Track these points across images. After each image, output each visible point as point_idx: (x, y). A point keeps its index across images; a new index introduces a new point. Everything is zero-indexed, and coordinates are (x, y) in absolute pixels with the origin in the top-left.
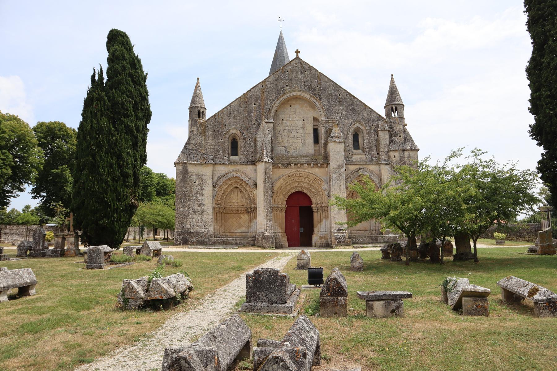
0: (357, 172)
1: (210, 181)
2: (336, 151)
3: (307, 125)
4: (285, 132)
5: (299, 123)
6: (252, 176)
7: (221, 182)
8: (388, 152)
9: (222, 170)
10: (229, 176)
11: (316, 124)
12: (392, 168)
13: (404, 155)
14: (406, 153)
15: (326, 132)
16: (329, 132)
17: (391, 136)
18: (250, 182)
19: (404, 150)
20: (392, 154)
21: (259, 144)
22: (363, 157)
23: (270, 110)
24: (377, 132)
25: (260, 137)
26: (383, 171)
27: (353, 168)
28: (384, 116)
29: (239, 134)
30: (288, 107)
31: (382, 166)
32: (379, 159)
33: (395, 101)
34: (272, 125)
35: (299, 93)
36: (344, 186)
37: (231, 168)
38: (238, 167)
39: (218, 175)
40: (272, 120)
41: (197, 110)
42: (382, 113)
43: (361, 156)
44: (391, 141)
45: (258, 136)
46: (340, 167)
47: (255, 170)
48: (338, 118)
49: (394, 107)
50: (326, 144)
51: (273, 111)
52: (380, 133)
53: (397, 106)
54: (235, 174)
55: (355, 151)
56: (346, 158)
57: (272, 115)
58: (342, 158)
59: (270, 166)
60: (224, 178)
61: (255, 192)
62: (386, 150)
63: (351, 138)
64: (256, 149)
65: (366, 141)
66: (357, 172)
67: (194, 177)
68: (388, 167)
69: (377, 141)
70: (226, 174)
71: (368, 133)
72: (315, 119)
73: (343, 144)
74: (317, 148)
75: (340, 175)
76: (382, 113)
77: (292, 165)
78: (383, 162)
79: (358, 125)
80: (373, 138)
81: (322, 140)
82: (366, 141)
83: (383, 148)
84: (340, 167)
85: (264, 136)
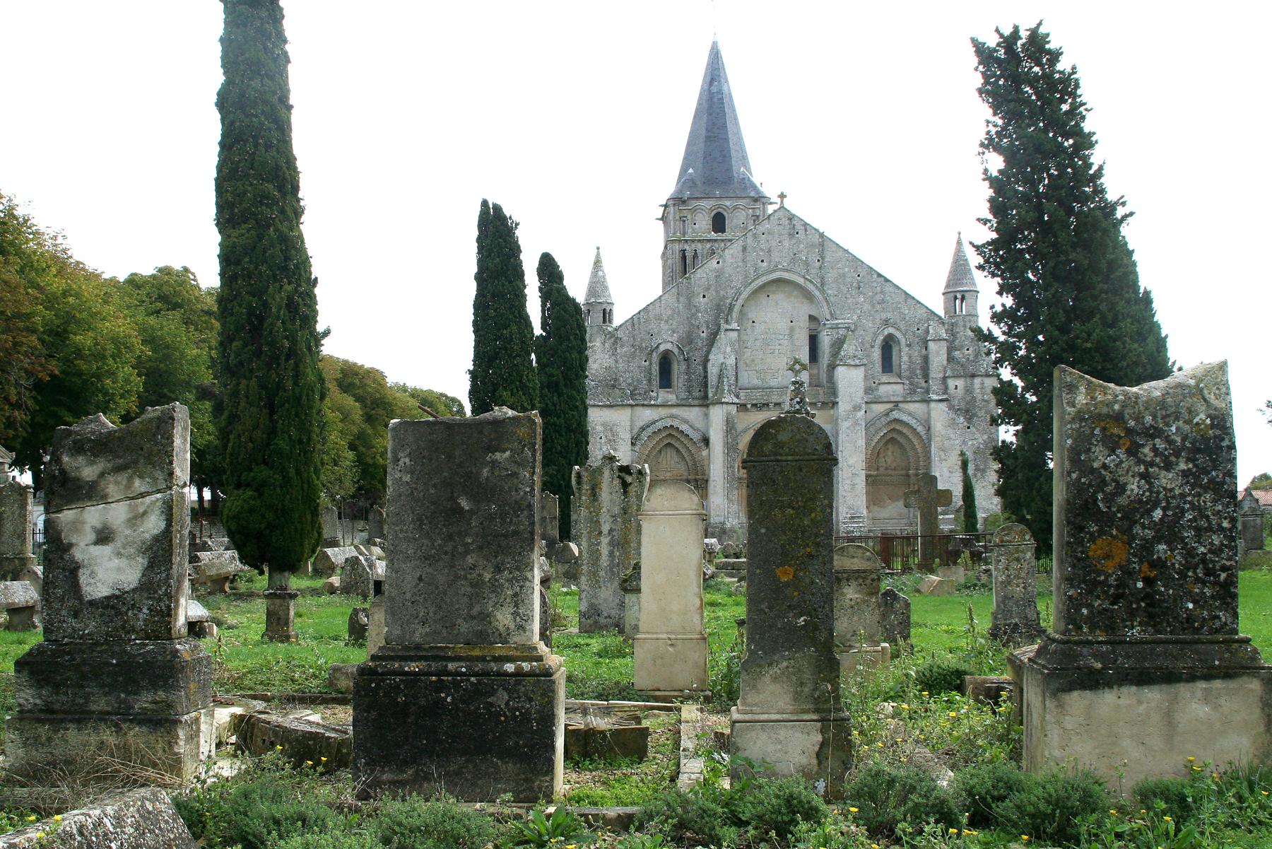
0: (887, 415)
1: (628, 436)
2: (850, 381)
3: (797, 330)
4: (758, 343)
5: (783, 325)
6: (699, 424)
7: (644, 436)
8: (945, 378)
9: (647, 415)
10: (659, 425)
11: (813, 326)
12: (951, 408)
13: (972, 384)
14: (977, 381)
15: (832, 346)
16: (838, 344)
17: (950, 350)
18: (695, 436)
19: (973, 376)
20: (951, 383)
21: (713, 370)
22: (899, 388)
23: (731, 307)
24: (925, 343)
25: (716, 359)
26: (933, 414)
27: (879, 408)
28: (941, 313)
29: (676, 351)
30: (762, 297)
31: (933, 405)
32: (927, 391)
33: (961, 284)
34: (735, 334)
35: (786, 275)
36: (861, 442)
37: (663, 412)
38: (675, 411)
39: (640, 424)
40: (734, 325)
41: (600, 308)
42: (938, 306)
43: (894, 386)
44: (950, 359)
45: (711, 357)
46: (856, 408)
47: (706, 415)
48: (855, 317)
49: (959, 296)
50: (832, 367)
51: (737, 309)
52: (931, 345)
53: (967, 295)
54: (669, 423)
55: (885, 378)
56: (868, 390)
57: (735, 315)
58: (861, 393)
59: (733, 409)
60: (650, 430)
61: (704, 453)
62: (941, 375)
63: (877, 354)
64: (706, 377)
65: (905, 358)
66: (887, 415)
67: (599, 428)
68: (943, 406)
69: (926, 359)
70: (654, 422)
71: (909, 346)
72: (812, 318)
73: (862, 369)
74: (815, 371)
75: (856, 423)
76: (938, 306)
77: (771, 406)
78: (935, 397)
79: (891, 330)
80: (916, 353)
81: (825, 359)
82: (905, 358)
83: (935, 373)
84: (856, 408)
85: (722, 356)
